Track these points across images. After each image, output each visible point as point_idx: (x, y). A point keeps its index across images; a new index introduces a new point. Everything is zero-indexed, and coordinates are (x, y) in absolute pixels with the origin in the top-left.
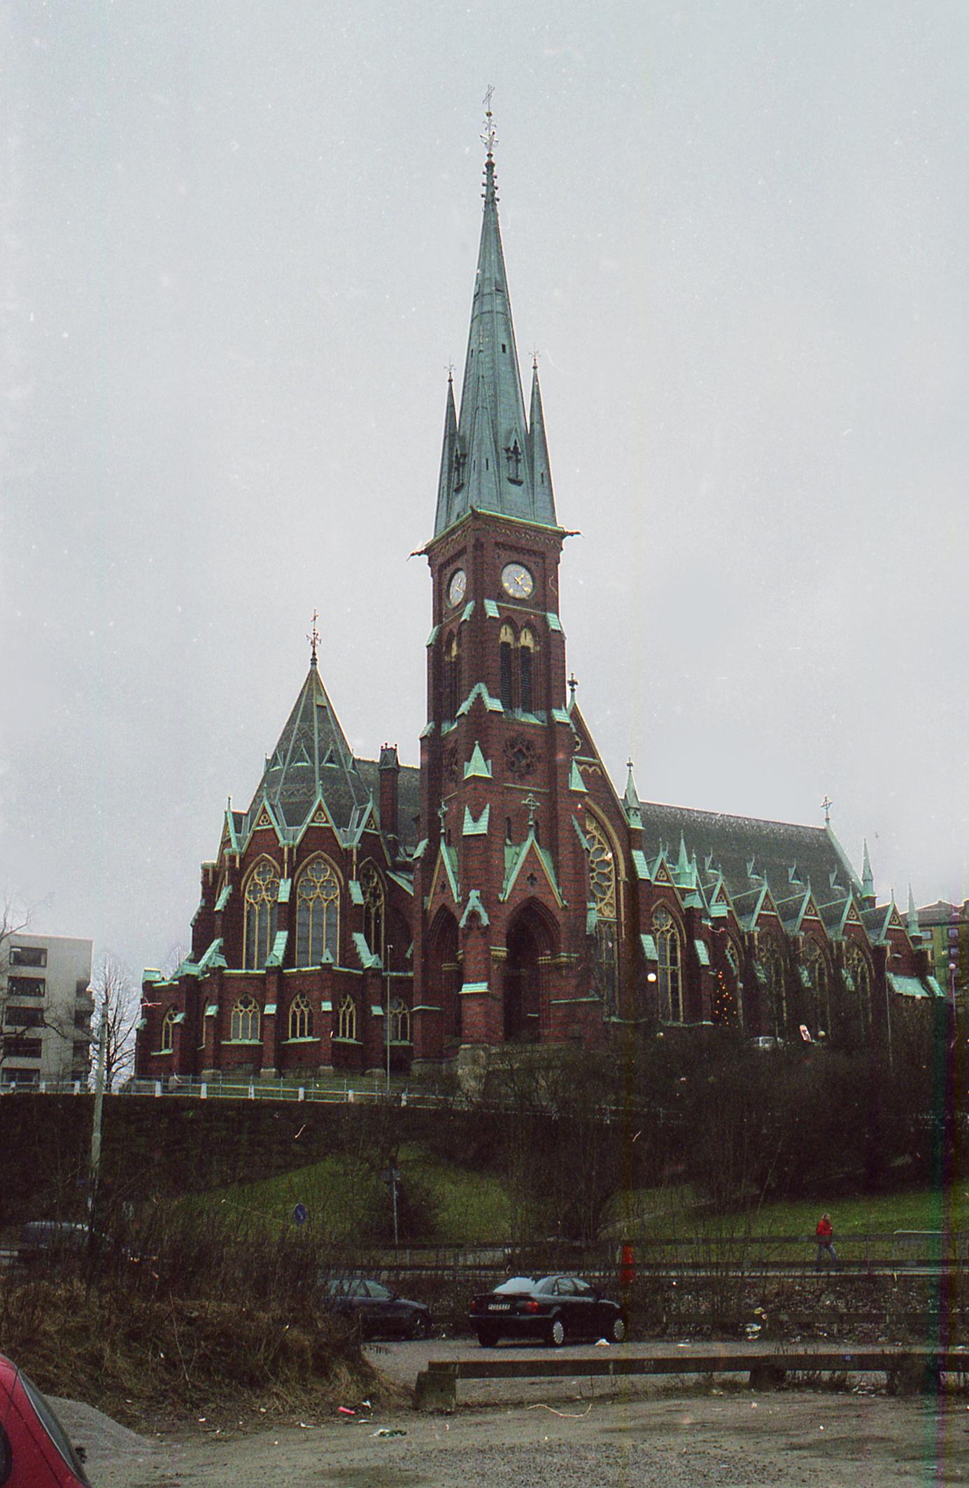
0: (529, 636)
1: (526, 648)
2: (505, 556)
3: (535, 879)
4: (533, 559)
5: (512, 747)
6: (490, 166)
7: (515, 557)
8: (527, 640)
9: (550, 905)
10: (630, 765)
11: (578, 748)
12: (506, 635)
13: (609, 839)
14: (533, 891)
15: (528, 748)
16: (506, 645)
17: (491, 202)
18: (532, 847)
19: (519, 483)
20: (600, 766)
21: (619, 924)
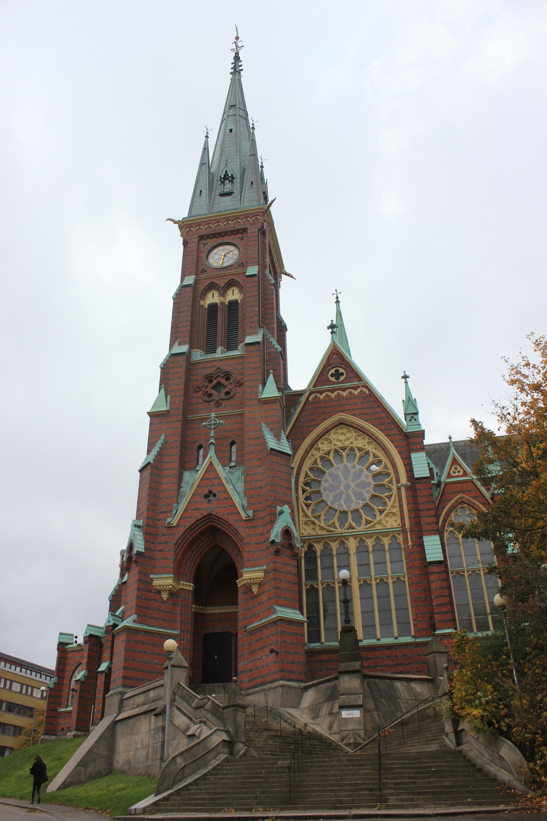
0: (236, 291)
1: (233, 304)
2: (211, 243)
3: (215, 495)
4: (239, 236)
5: (210, 381)
6: (237, 58)
7: (221, 240)
8: (234, 295)
9: (231, 520)
10: (405, 377)
11: (342, 378)
12: (213, 298)
13: (384, 449)
14: (207, 508)
15: (228, 379)
16: (213, 307)
17: (236, 70)
18: (211, 463)
19: (230, 194)
20: (367, 386)
21: (404, 530)
